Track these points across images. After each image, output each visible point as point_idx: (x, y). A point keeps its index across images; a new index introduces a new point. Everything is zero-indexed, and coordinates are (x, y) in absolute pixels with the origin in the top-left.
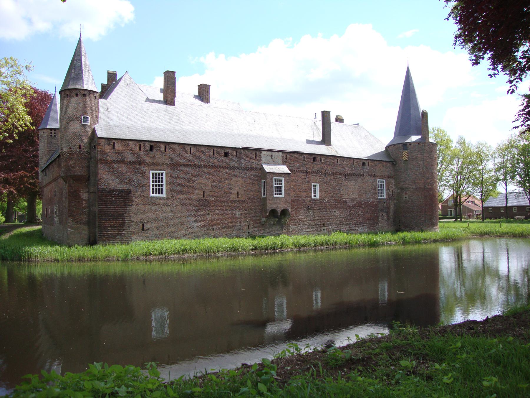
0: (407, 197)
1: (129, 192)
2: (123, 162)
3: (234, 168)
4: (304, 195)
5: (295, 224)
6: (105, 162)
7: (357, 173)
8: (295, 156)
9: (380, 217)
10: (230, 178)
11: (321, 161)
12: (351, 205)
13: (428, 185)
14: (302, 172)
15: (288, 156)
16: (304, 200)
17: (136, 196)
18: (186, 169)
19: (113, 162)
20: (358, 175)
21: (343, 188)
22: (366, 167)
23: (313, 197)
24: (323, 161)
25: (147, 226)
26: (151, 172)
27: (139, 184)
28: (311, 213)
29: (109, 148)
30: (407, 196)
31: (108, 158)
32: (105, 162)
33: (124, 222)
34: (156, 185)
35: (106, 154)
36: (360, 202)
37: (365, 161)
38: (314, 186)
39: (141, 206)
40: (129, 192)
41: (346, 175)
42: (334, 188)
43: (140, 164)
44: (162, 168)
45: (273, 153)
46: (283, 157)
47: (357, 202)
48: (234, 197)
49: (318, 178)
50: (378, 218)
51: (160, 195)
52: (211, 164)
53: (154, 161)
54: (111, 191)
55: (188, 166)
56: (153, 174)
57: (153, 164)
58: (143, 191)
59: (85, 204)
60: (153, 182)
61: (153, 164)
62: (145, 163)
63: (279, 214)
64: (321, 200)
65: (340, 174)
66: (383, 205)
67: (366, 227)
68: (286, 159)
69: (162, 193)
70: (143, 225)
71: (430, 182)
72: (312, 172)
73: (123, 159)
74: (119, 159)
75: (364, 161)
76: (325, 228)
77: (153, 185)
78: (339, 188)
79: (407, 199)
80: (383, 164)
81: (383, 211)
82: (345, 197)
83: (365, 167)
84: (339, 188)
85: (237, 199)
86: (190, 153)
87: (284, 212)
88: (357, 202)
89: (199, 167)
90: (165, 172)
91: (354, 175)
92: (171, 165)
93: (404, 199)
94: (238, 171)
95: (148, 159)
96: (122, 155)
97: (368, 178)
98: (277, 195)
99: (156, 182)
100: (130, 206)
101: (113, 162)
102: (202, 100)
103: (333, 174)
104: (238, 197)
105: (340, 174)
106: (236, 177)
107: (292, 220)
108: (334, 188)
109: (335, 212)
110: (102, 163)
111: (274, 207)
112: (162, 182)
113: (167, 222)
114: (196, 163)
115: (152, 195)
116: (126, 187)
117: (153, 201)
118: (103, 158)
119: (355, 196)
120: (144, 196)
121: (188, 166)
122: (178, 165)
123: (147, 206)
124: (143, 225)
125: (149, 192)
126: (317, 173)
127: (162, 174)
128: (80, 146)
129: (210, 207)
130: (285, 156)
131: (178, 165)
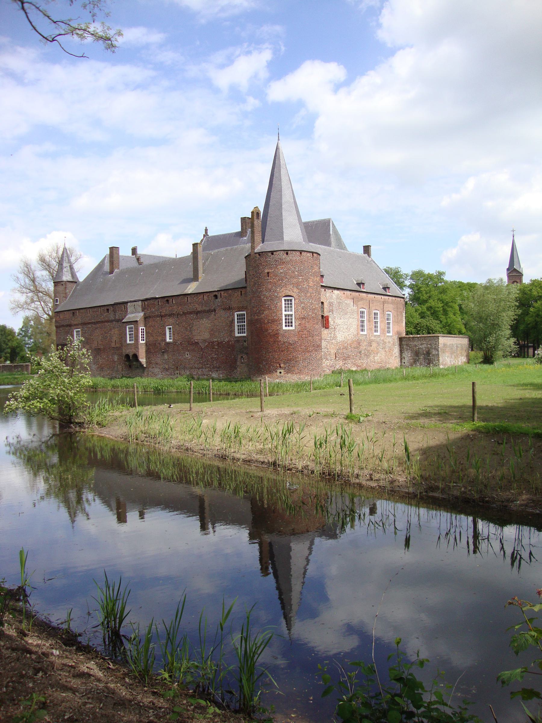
3: (112, 321)
4: (160, 339)
5: (153, 367)
7: (207, 309)
8: (152, 301)
9: (239, 360)
12: (203, 347)
13: (254, 316)
16: (160, 344)
20: (210, 311)
22: (219, 299)
24: (174, 302)
28: (166, 357)
36: (213, 342)
37: (216, 293)
41: (197, 313)
44: (78, 327)
46: (142, 305)
47: (209, 343)
48: (113, 345)
49: (171, 320)
50: (236, 361)
52: (100, 320)
55: (89, 323)
64: (174, 343)
65: (191, 313)
66: (243, 345)
67: (221, 372)
71: (256, 310)
72: (165, 315)
75: (215, 293)
76: (178, 372)
78: (190, 328)
80: (241, 291)
82: (197, 338)
83: (217, 300)
84: (190, 328)
88: (209, 343)
89: (94, 323)
91: (204, 311)
94: (114, 323)
97: (221, 314)
98: (241, 333)
103: (184, 314)
105: (191, 313)
108: (186, 328)
114: (93, 321)
119: (206, 336)
121: (89, 323)
130: (144, 304)
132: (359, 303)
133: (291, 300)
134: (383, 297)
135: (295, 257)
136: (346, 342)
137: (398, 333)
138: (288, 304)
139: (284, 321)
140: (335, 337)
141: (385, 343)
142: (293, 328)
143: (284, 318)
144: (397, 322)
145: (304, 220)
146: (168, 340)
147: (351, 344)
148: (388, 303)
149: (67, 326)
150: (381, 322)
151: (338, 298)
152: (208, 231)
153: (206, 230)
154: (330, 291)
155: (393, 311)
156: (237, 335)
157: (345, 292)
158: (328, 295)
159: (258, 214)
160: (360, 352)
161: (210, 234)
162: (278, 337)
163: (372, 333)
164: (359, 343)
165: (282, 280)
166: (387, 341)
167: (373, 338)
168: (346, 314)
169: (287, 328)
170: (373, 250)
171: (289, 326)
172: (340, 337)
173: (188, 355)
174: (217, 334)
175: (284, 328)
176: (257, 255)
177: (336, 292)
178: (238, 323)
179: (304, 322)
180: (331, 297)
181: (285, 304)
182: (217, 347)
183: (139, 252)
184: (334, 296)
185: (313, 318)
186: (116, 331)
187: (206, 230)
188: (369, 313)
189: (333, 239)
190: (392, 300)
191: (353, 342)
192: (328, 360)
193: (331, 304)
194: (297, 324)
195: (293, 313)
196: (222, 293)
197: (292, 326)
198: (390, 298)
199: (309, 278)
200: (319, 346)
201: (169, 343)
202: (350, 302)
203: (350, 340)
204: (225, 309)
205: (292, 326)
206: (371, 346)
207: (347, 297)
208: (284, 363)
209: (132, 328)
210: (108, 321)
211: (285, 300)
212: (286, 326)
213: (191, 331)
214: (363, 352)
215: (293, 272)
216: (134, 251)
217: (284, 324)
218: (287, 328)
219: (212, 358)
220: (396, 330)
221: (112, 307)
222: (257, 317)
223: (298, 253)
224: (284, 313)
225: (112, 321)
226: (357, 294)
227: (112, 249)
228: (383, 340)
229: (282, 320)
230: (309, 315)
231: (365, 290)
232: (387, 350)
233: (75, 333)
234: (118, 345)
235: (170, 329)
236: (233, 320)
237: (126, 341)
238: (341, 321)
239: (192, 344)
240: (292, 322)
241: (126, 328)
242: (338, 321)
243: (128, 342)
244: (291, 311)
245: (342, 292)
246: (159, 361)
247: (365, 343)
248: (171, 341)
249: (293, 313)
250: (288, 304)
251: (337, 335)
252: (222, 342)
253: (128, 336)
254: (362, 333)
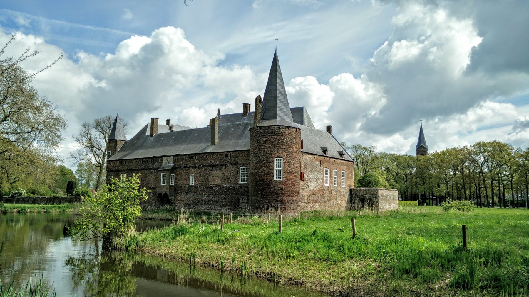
3: (150, 169)
4: (185, 183)
8: (180, 157)
9: (241, 200)
10: (149, 175)
11: (195, 158)
13: (254, 170)
14: (184, 167)
15: (176, 158)
16: (184, 187)
20: (222, 165)
21: (210, 176)
24: (197, 158)
28: (188, 196)
36: (223, 187)
37: (227, 153)
45: (168, 158)
46: (173, 159)
47: (220, 187)
64: (195, 187)
66: (244, 190)
68: (175, 160)
71: (256, 166)
72: (190, 167)
75: (226, 153)
76: (197, 207)
80: (245, 153)
81: (244, 195)
82: (212, 184)
83: (227, 158)
88: (220, 187)
91: (218, 165)
97: (229, 167)
103: (204, 166)
105: (208, 166)
106: (151, 174)
108: (204, 176)
109: (204, 195)
114: (136, 168)
119: (219, 182)
126: (194, 167)
132: (324, 164)
133: (281, 160)
134: (340, 161)
135: (285, 131)
136: (315, 191)
137: (350, 186)
138: (279, 162)
139: (275, 174)
140: (308, 187)
141: (340, 192)
142: (281, 179)
143: (275, 172)
144: (349, 178)
145: (291, 106)
146: (191, 184)
147: (318, 192)
148: (343, 165)
149: (116, 171)
150: (339, 177)
151: (310, 160)
152: (220, 112)
153: (219, 111)
154: (306, 155)
155: (346, 171)
156: (240, 182)
157: (315, 156)
158: (304, 158)
159: (260, 99)
160: (324, 198)
161: (221, 113)
162: (270, 185)
163: (333, 185)
164: (324, 192)
165: (275, 146)
166: (342, 191)
167: (333, 188)
168: (316, 171)
169: (278, 179)
170: (333, 130)
171: (278, 178)
172: (311, 187)
173: (205, 196)
174: (226, 181)
175: (275, 179)
176: (258, 128)
177: (310, 156)
178: (241, 174)
179: (289, 175)
180: (306, 160)
181: (277, 162)
182: (225, 190)
183: (172, 123)
184: (308, 159)
185: (295, 172)
186: (152, 177)
187: (219, 111)
188: (331, 171)
189: (306, 121)
190: (346, 163)
191: (320, 190)
192: (303, 203)
193: (306, 164)
194: (285, 176)
195: (281, 169)
196: (232, 153)
197: (280, 178)
198: (345, 161)
199: (293, 146)
200: (299, 193)
201: (190, 187)
202: (318, 163)
203: (318, 190)
204: (233, 164)
205: (280, 178)
206: (331, 194)
207: (317, 160)
208: (274, 203)
209: (165, 175)
210: (147, 169)
211: (277, 160)
212: (276, 178)
213: (207, 178)
214: (326, 198)
215: (283, 141)
216: (168, 121)
218: (278, 179)
219: (221, 198)
220: (348, 183)
221: (151, 160)
222: (256, 171)
223: (287, 129)
224: (276, 168)
225: (150, 169)
226: (323, 158)
227: (153, 119)
228: (339, 190)
229: (274, 173)
230: (292, 171)
231: (328, 156)
232: (342, 197)
234: (153, 186)
235: (192, 176)
236: (238, 172)
237: (160, 183)
238: (312, 176)
240: (280, 175)
241: (160, 174)
242: (310, 176)
243: (162, 184)
244: (281, 167)
245: (313, 156)
246: (183, 199)
247: (328, 192)
248: (193, 185)
249: (281, 169)
250: (279, 162)
251: (309, 186)
252: (229, 187)
253: (162, 180)
254: (325, 185)
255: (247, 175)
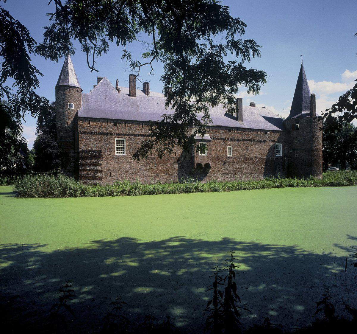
0: (298, 156)
1: (100, 152)
2: (96, 133)
6: (84, 133)
17: (104, 155)
18: (139, 137)
19: (89, 133)
23: (228, 156)
25: (113, 174)
26: (116, 139)
27: (107, 147)
29: (85, 124)
30: (298, 154)
31: (85, 130)
32: (84, 133)
33: (97, 172)
34: (119, 148)
35: (84, 128)
38: (230, 148)
39: (108, 161)
40: (100, 152)
41: (252, 141)
42: (244, 149)
43: (107, 134)
47: (260, 159)
49: (232, 143)
51: (122, 154)
53: (117, 132)
54: (88, 152)
56: (117, 141)
57: (117, 134)
58: (111, 152)
59: (72, 160)
60: (117, 145)
61: (117, 134)
62: (112, 134)
63: (203, 167)
64: (234, 157)
69: (123, 153)
70: (110, 173)
72: (228, 139)
73: (96, 131)
74: (93, 131)
76: (236, 176)
77: (117, 148)
79: (298, 156)
82: (251, 155)
83: (267, 135)
85: (175, 157)
86: (142, 127)
87: (207, 166)
88: (260, 159)
90: (125, 139)
92: (129, 135)
93: (296, 156)
95: (113, 131)
96: (95, 128)
99: (119, 146)
100: (102, 161)
101: (89, 133)
102: (145, 93)
103: (243, 140)
104: (175, 155)
105: (248, 140)
107: (213, 170)
108: (244, 149)
109: (244, 165)
110: (81, 133)
111: (200, 161)
112: (123, 146)
113: (127, 172)
115: (116, 154)
116: (99, 149)
117: (116, 158)
118: (83, 130)
120: (110, 155)
122: (134, 135)
123: (114, 161)
124: (110, 173)
125: (114, 152)
126: (232, 140)
127: (123, 141)
128: (67, 122)
129: (156, 162)
131: (134, 135)
173: (245, 166)
217: (116, 151)
233: (116, 142)
239: (248, 159)
255: (276, 150)
